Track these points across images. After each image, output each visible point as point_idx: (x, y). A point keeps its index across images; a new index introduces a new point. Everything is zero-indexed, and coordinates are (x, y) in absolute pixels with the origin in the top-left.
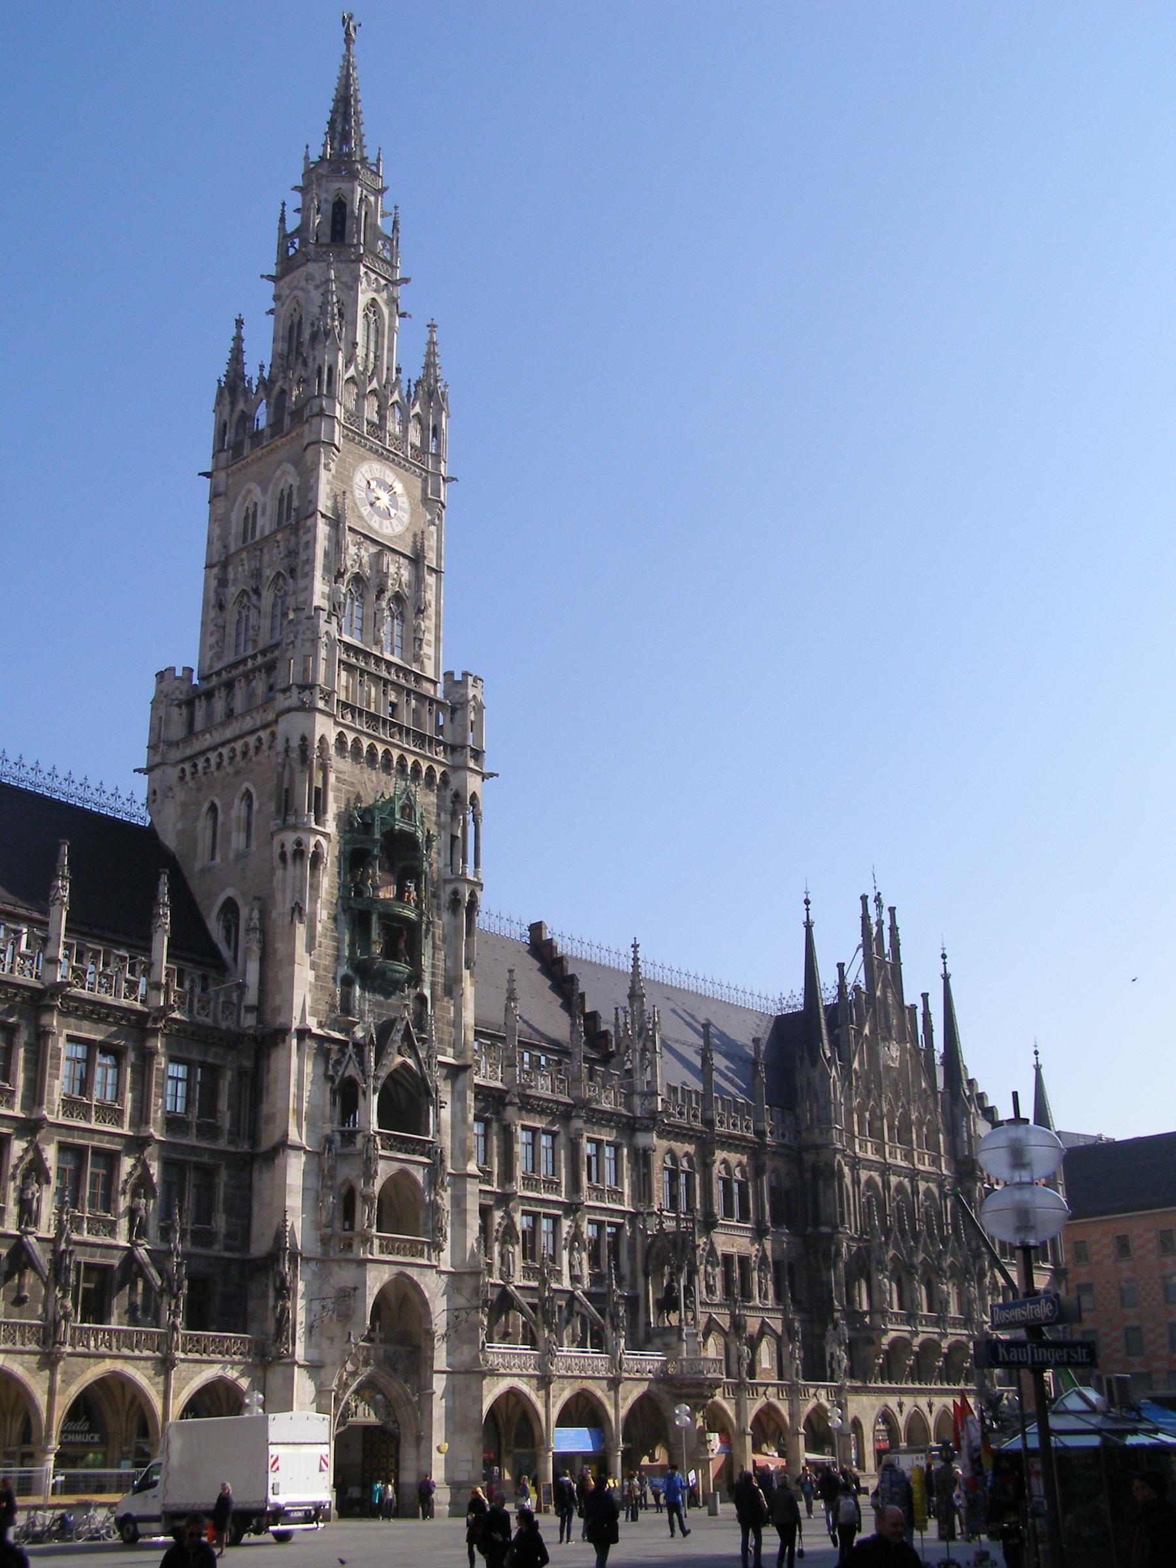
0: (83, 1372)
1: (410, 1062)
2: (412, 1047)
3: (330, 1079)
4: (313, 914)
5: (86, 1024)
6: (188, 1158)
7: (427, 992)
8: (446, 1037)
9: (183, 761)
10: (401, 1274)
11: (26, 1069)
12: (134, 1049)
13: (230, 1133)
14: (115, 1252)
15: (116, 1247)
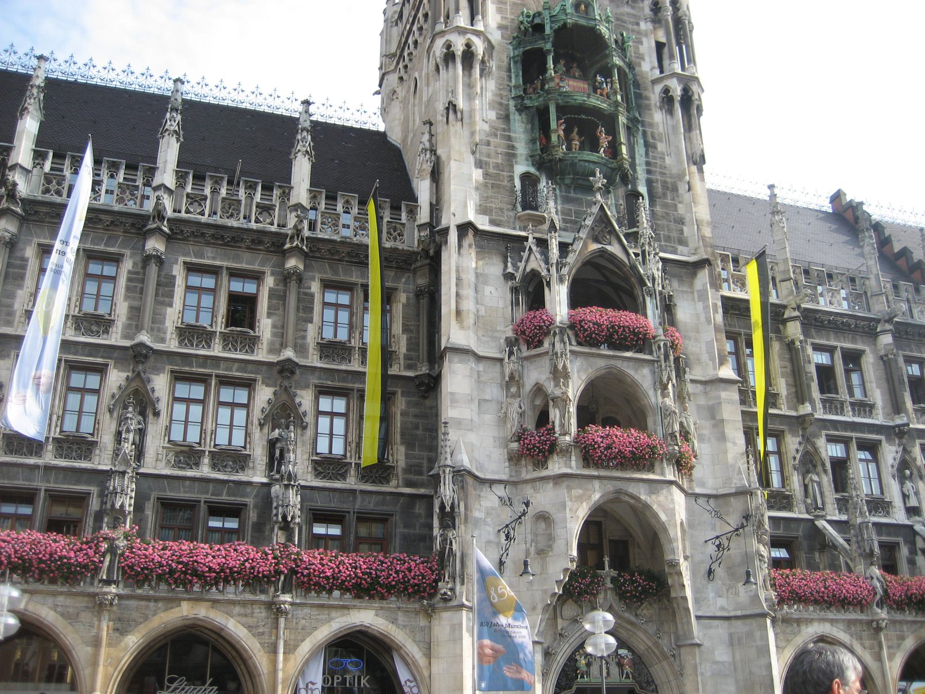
0: (146, 618)
1: (614, 249)
2: (613, 232)
3: (509, 277)
4: (472, 112)
5: (209, 251)
6: (350, 385)
7: (643, 189)
8: (674, 234)
9: (398, 63)
10: (619, 492)
11: (127, 298)
12: (272, 274)
13: (407, 357)
14: (249, 489)
15: (250, 483)
